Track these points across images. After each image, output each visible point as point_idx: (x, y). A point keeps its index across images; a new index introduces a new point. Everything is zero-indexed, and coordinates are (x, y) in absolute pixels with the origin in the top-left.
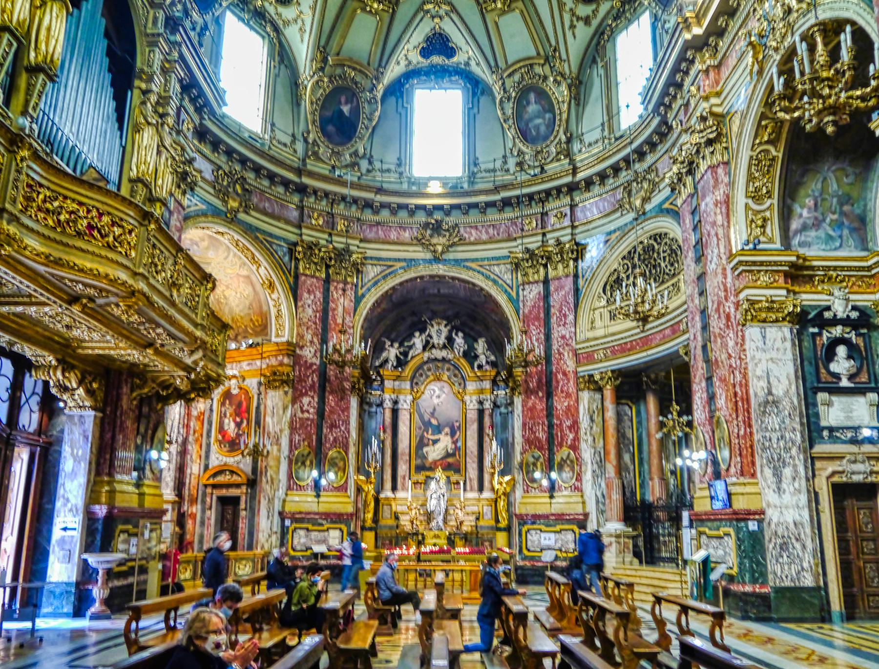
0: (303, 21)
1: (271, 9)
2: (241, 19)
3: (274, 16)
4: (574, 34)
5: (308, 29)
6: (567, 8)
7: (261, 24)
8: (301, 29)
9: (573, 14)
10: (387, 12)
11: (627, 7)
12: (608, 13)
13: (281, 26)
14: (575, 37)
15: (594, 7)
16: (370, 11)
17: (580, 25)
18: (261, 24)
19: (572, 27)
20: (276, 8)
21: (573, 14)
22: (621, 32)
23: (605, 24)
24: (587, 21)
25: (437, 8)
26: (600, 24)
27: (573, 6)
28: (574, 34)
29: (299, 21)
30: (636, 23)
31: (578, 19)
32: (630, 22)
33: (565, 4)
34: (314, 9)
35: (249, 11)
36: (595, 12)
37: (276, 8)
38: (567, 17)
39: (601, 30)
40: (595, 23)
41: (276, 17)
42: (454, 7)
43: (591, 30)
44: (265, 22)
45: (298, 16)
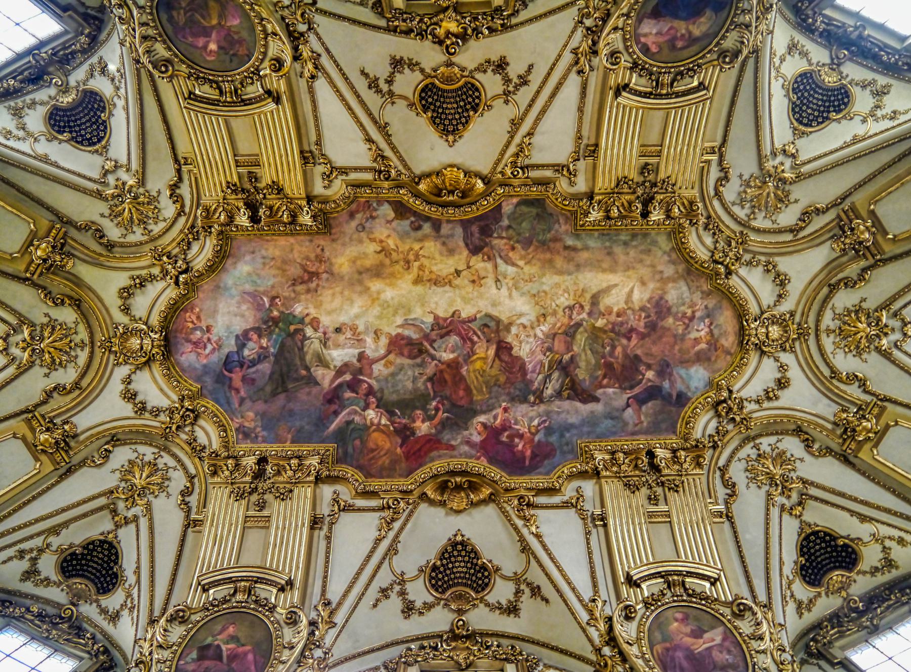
0: (24, 139)
1: (42, 95)
2: (42, 44)
3: (31, 96)
4: (10, 559)
5: (11, 143)
6: (51, 539)
7: (21, 73)
8: (10, 132)
9: (41, 551)
10: (27, 270)
11: (65, 626)
12: (48, 602)
13: (12, 104)
14: (4, 562)
15: (54, 577)
16: (31, 244)
17: (25, 565)
18: (21, 73)
19: (21, 554)
20: (42, 103)
21: (41, 551)
22: (22, 631)
23: (28, 602)
24: (30, 574)
25: (21, 345)
26: (26, 596)
27: (54, 548)
28: (10, 559)
29: (21, 133)
30: (46, 651)
31: (34, 561)
32: (45, 641)
33: (58, 534)
34: (45, 159)
35: (50, 62)
36: (47, 582)
37: (42, 103)
38: (38, 542)
39: (14, 599)
40: (28, 587)
41: (28, 99)
42: (26, 370)
43: (15, 585)
44: (22, 82)
45: (30, 134)
